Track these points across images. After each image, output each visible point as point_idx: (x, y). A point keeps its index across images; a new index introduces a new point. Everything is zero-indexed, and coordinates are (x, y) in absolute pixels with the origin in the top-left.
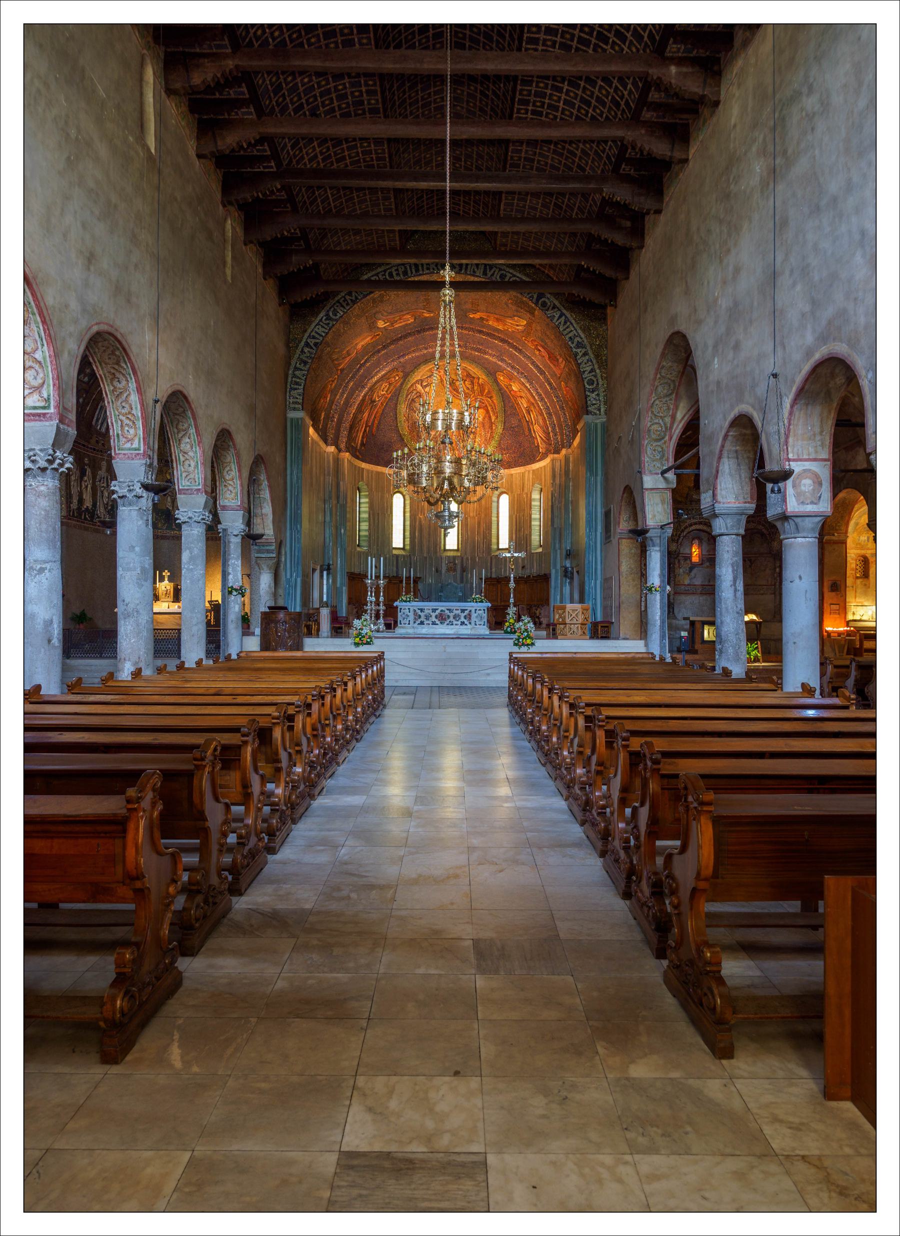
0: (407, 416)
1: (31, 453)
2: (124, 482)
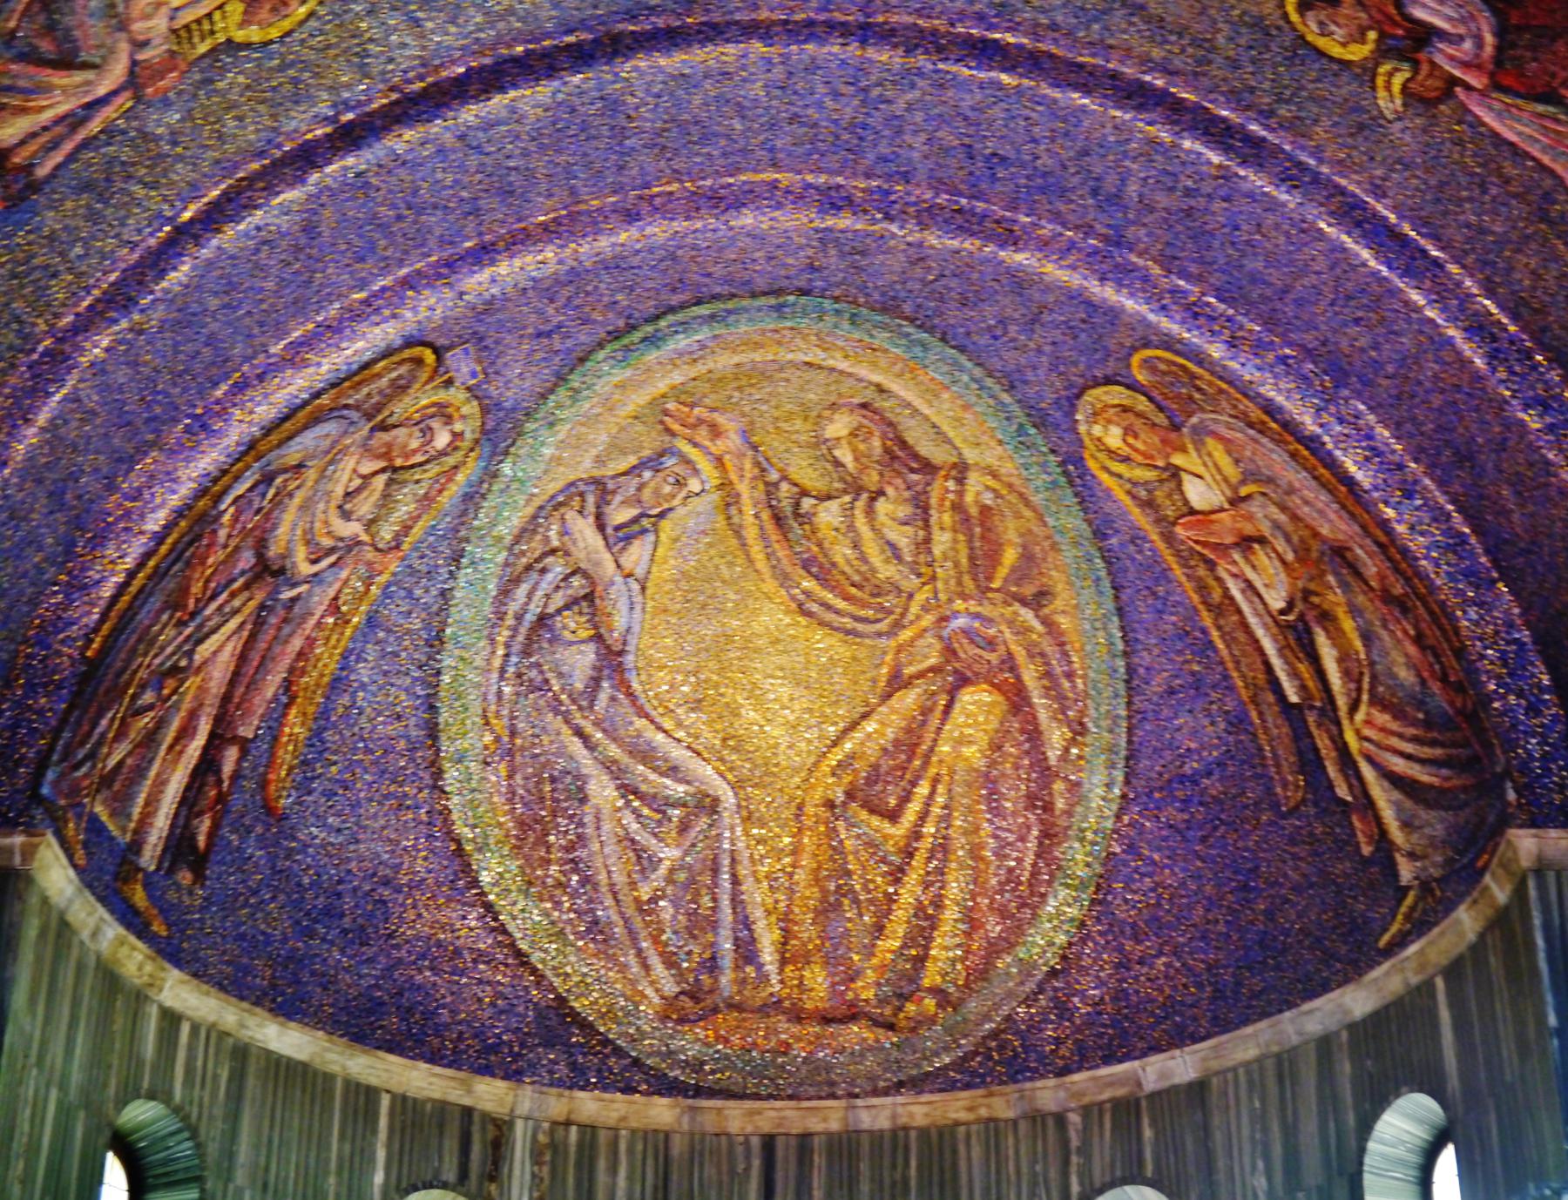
0: (500, 725)
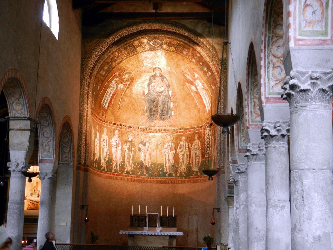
1: (278, 125)
2: (256, 144)
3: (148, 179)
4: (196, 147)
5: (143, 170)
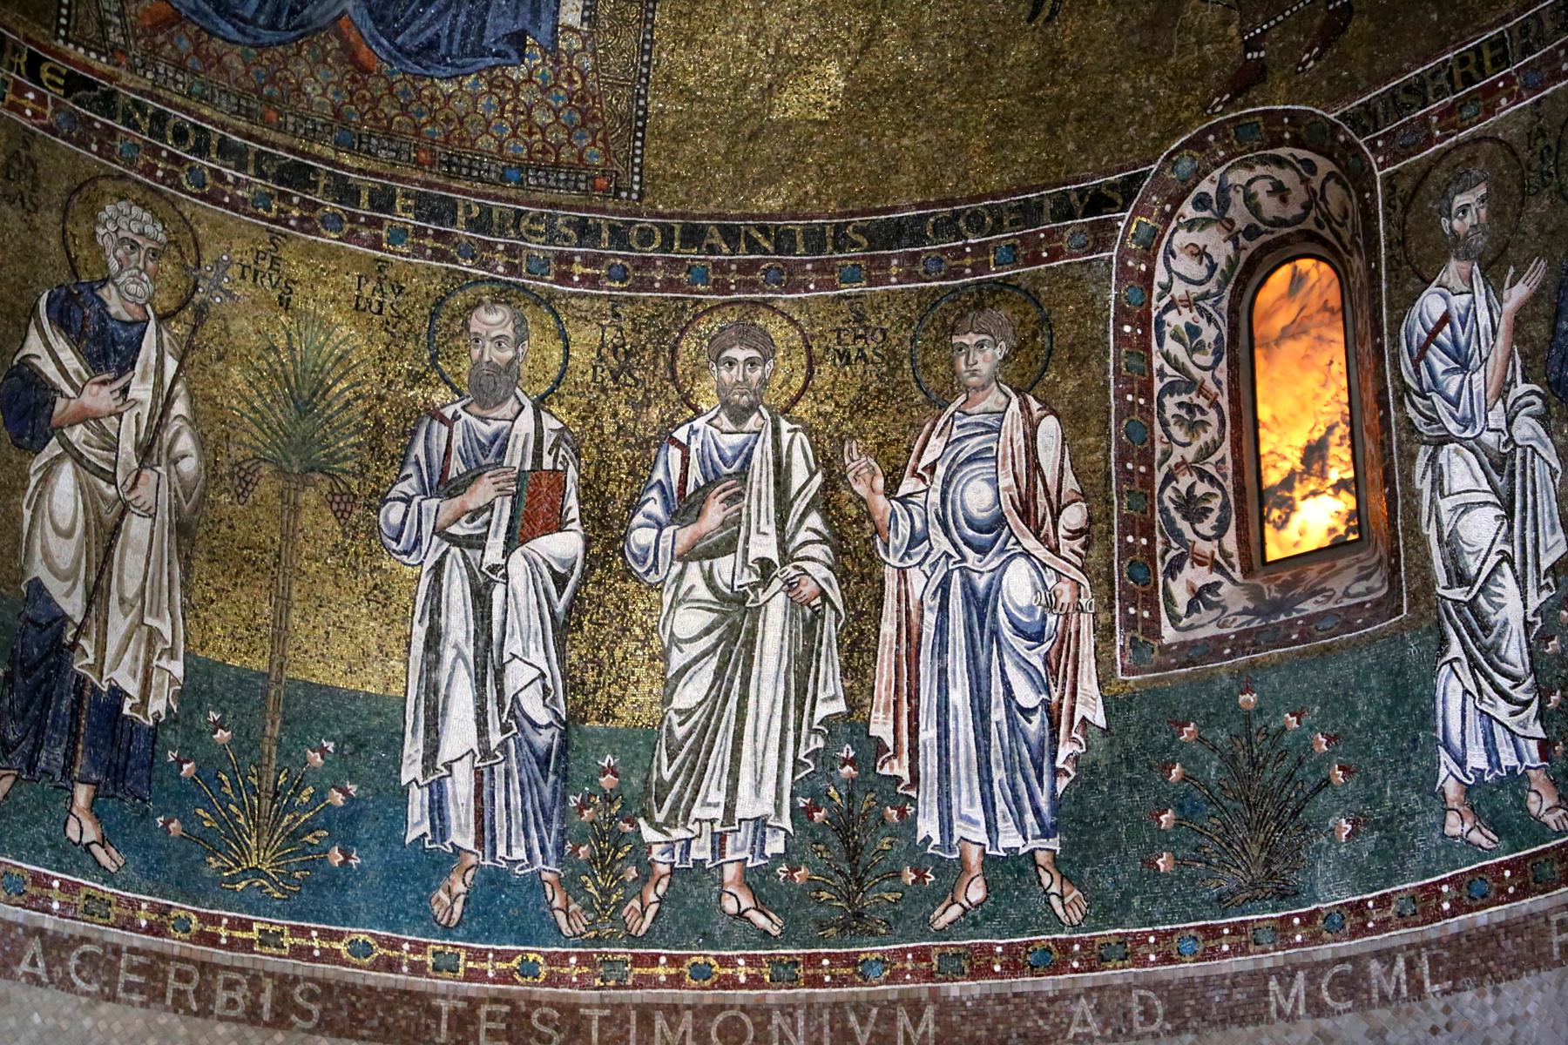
3: (115, 935)
4: (977, 497)
5: (52, 756)
